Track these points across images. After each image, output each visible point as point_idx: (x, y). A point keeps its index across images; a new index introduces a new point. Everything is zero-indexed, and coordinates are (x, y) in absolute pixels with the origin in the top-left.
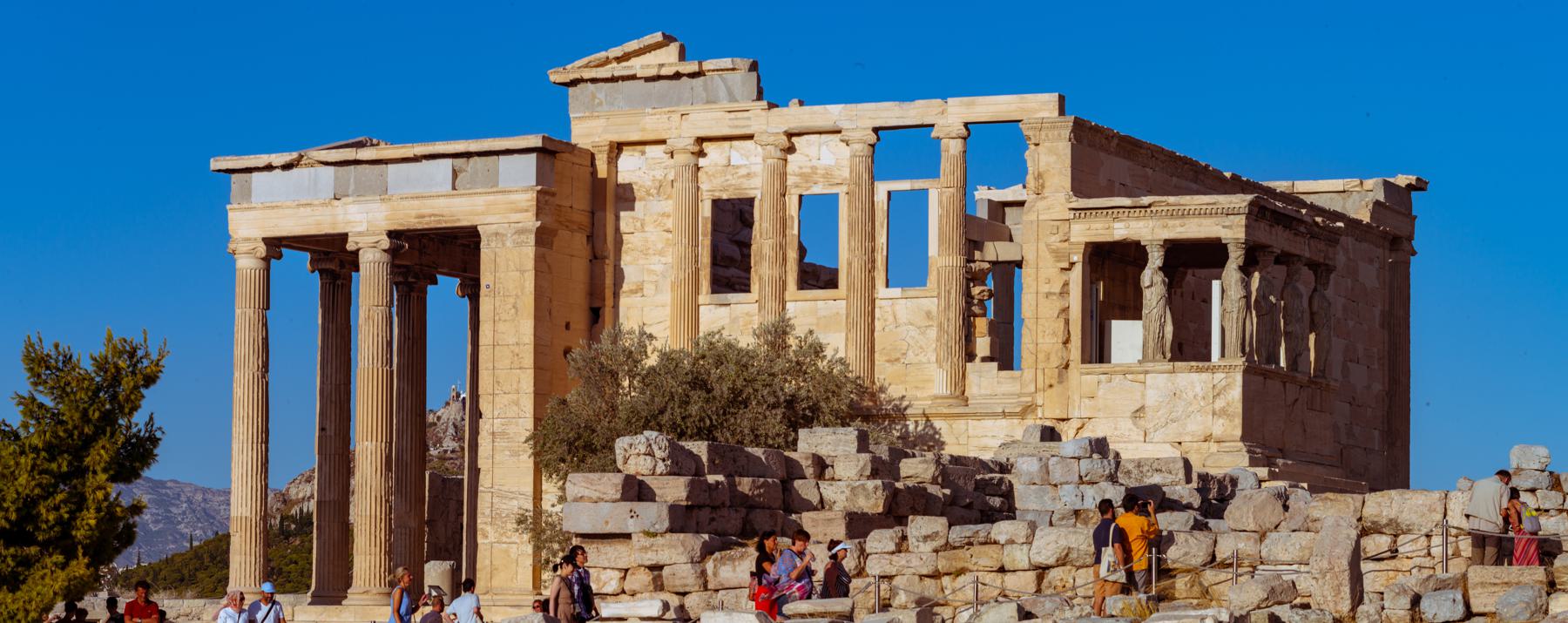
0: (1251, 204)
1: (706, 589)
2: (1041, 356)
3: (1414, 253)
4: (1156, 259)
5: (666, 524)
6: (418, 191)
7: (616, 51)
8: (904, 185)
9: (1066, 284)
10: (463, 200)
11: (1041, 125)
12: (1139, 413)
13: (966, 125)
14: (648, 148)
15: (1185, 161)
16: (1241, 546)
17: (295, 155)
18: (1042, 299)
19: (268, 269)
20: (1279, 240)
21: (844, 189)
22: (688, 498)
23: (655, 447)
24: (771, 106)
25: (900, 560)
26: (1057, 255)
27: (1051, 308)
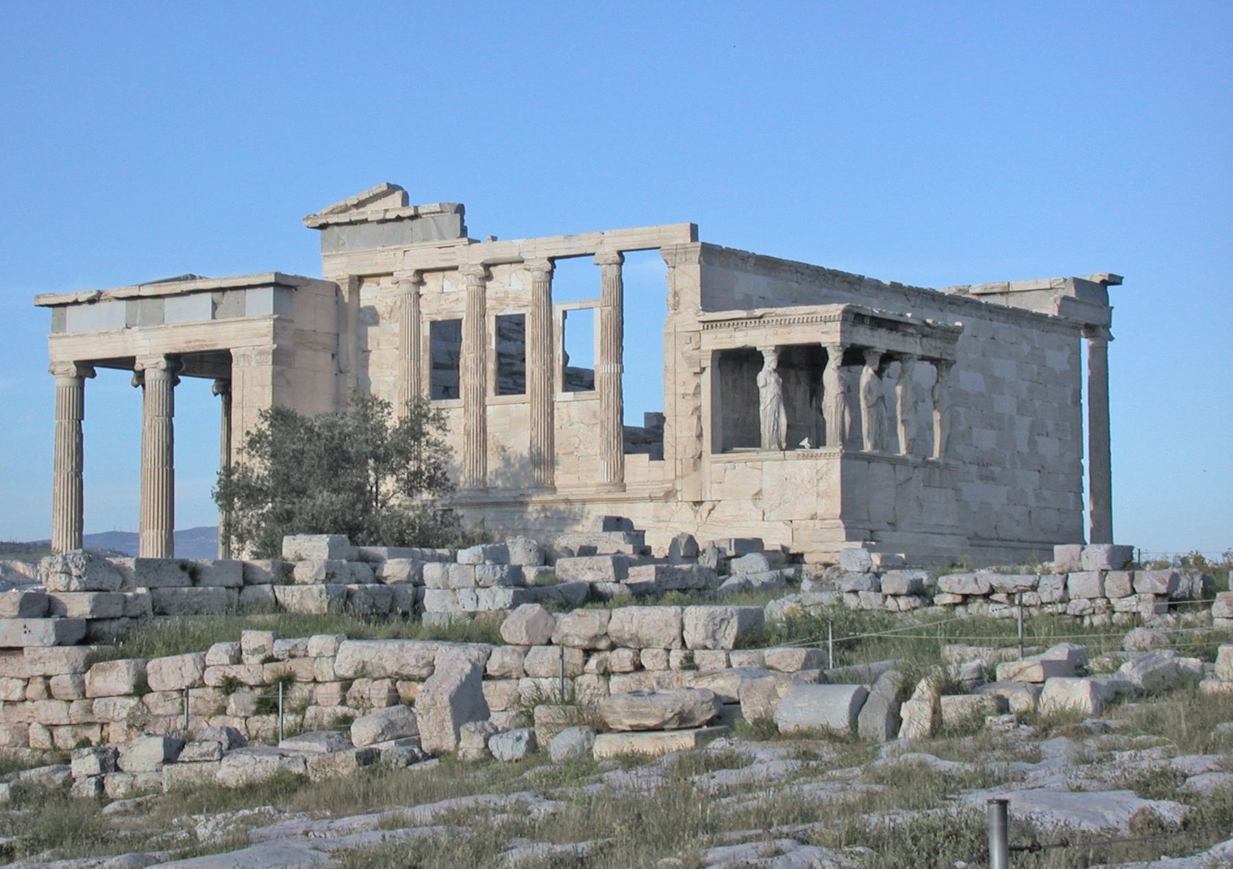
0: (845, 312)
1: (85, 697)
2: (680, 448)
3: (1112, 339)
4: (770, 362)
5: (53, 639)
9: (698, 386)
10: (221, 327)
12: (758, 495)
13: (620, 253)
14: (383, 280)
15: (835, 274)
16: (507, 659)
19: (81, 388)
20: (882, 341)
22: (92, 612)
23: (71, 566)
24: (471, 242)
26: (690, 361)
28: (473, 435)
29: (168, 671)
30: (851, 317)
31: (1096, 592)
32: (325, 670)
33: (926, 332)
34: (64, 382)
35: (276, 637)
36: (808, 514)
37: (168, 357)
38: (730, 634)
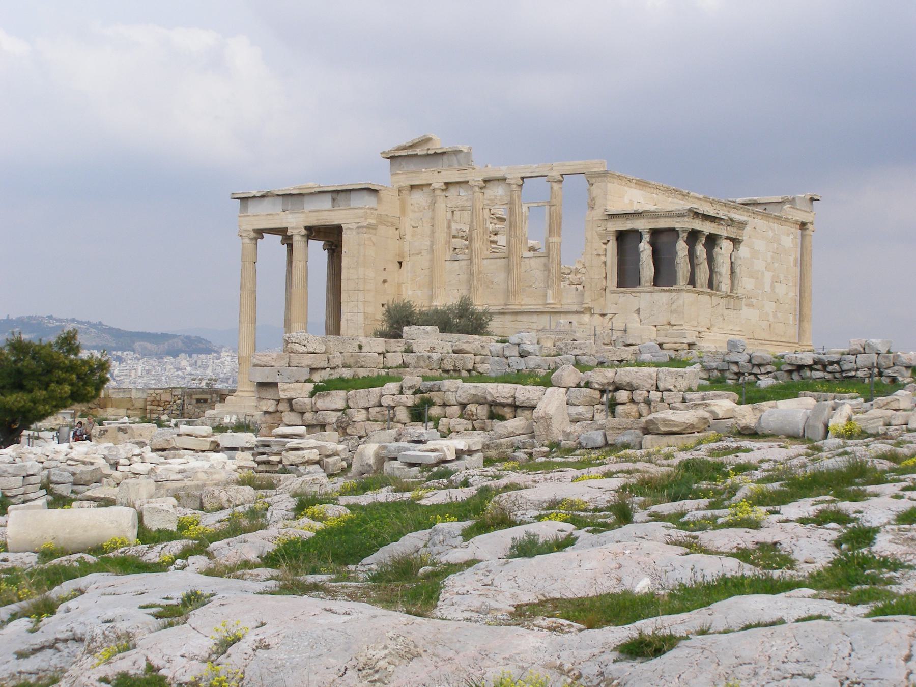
4: (646, 237)
19: (256, 244)
25: (398, 398)
26: (601, 236)
32: (451, 398)
33: (731, 222)
37: (306, 228)
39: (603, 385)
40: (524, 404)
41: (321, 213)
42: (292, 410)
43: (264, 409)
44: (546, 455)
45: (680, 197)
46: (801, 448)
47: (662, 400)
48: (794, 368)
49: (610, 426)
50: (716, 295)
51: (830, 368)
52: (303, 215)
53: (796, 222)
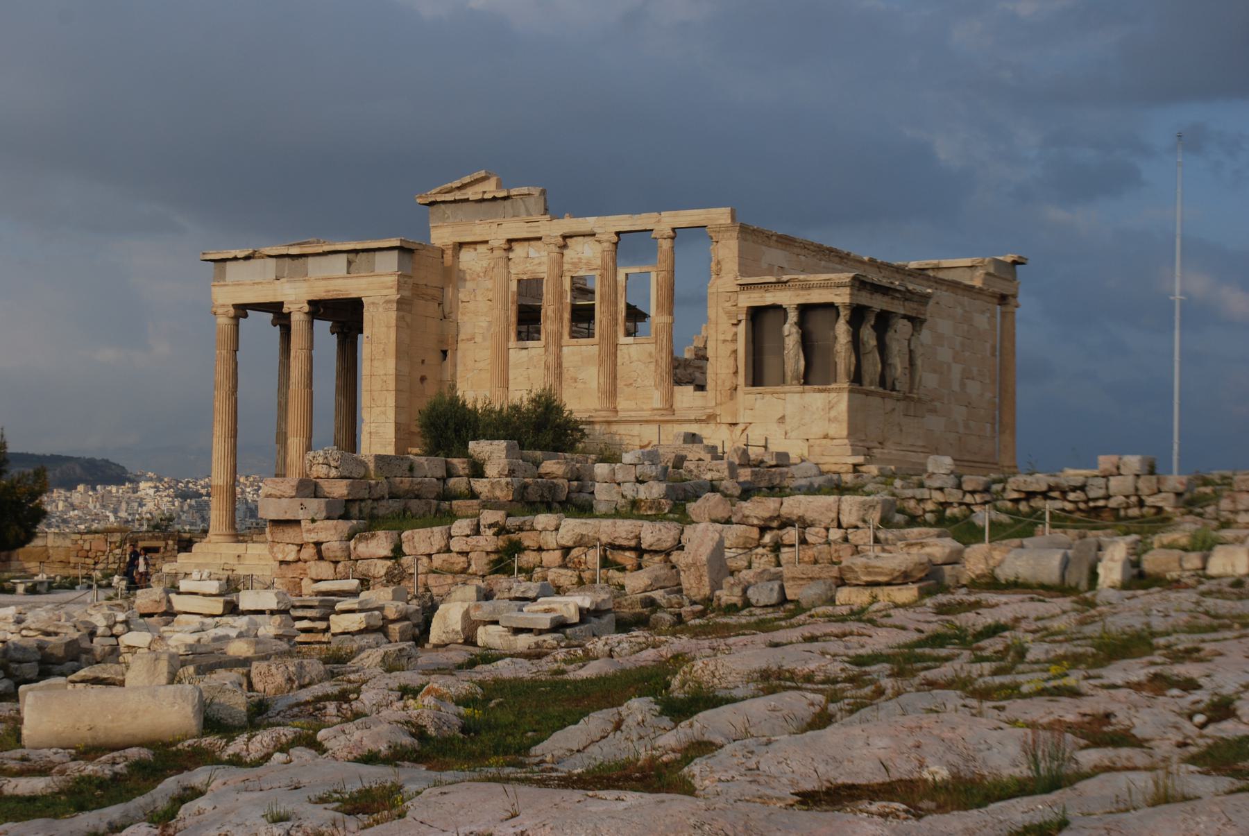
0: (854, 278)
4: (793, 317)
5: (324, 514)
6: (326, 275)
7: (457, 183)
8: (636, 270)
10: (353, 281)
11: (721, 229)
12: (782, 419)
13: (674, 229)
14: (478, 247)
15: (831, 250)
17: (251, 251)
18: (720, 344)
19: (237, 325)
20: (878, 303)
21: (598, 272)
25: (473, 540)
26: (729, 314)
27: (725, 350)
28: (552, 369)
29: (421, 540)
30: (857, 284)
31: (1132, 490)
32: (550, 540)
33: (908, 296)
34: (223, 321)
35: (508, 515)
36: (821, 434)
37: (310, 302)
38: (875, 517)
39: (765, 520)
40: (653, 548)
41: (333, 282)
42: (321, 558)
43: (280, 557)
44: (702, 614)
45: (837, 259)
46: (1066, 603)
47: (846, 540)
48: (1023, 496)
49: (790, 575)
50: (890, 397)
51: (1072, 496)
52: (305, 285)
53: (993, 295)
